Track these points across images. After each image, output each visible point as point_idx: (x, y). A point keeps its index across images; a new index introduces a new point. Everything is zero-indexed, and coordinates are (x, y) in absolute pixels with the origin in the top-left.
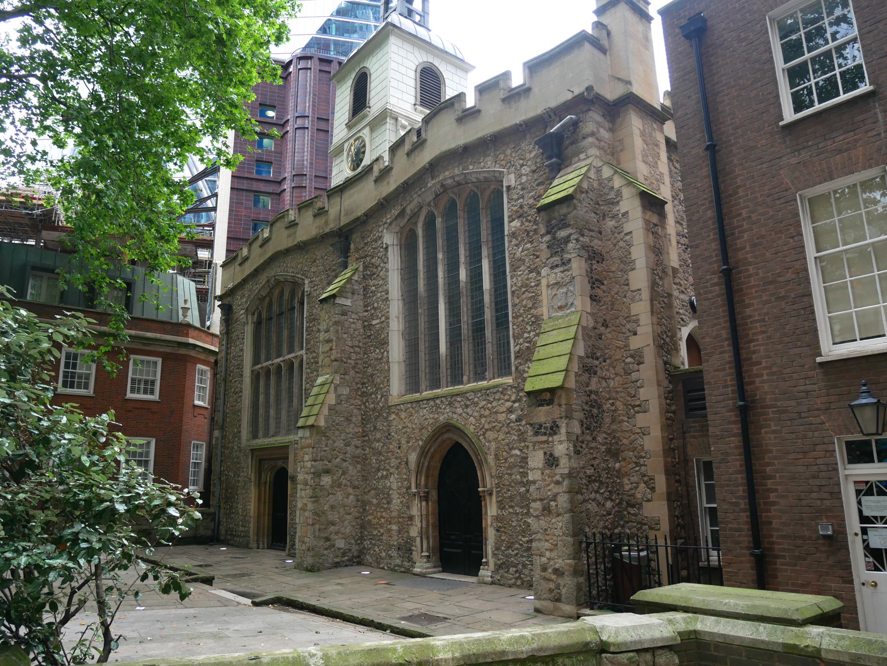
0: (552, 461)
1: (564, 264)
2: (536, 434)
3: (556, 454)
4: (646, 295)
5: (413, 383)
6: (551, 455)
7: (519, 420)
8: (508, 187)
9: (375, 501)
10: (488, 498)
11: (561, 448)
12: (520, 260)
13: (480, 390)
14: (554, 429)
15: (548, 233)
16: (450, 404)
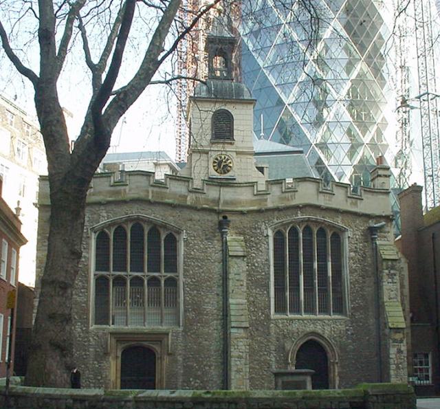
0: (400, 351)
1: (393, 283)
2: (394, 342)
3: (402, 349)
4: (408, 298)
5: (280, 308)
6: (400, 350)
7: (352, 334)
8: (349, 237)
9: (257, 367)
10: (336, 365)
11: (404, 348)
12: (355, 269)
13: (332, 320)
14: (401, 341)
15: (387, 269)
16: (313, 323)
